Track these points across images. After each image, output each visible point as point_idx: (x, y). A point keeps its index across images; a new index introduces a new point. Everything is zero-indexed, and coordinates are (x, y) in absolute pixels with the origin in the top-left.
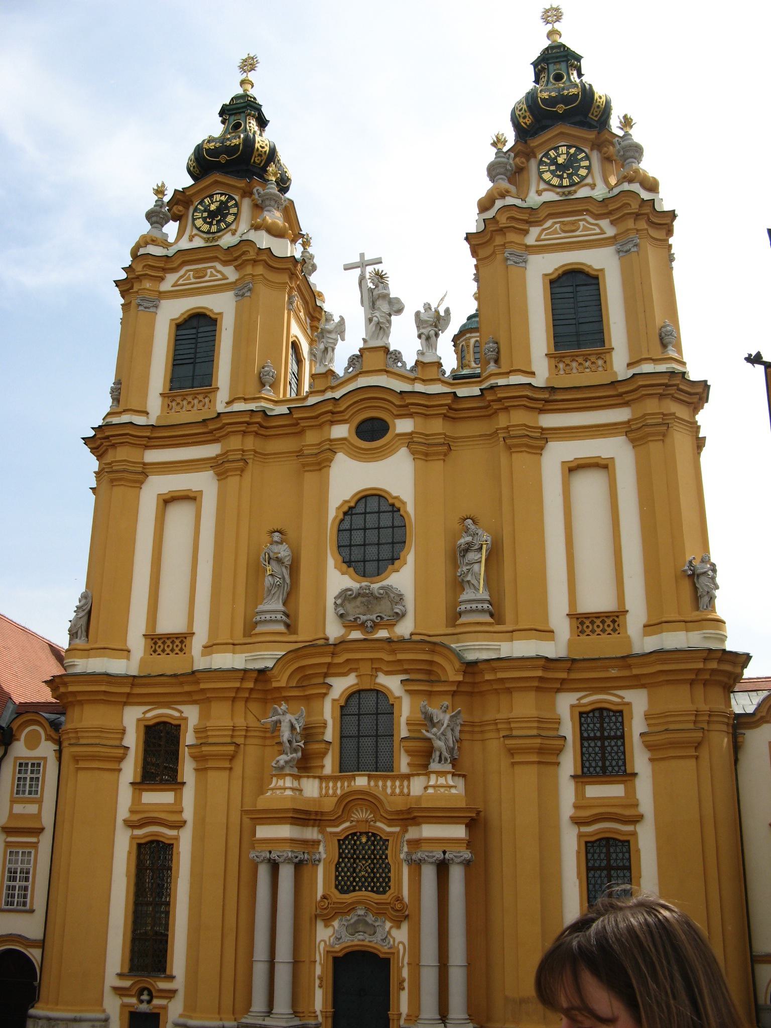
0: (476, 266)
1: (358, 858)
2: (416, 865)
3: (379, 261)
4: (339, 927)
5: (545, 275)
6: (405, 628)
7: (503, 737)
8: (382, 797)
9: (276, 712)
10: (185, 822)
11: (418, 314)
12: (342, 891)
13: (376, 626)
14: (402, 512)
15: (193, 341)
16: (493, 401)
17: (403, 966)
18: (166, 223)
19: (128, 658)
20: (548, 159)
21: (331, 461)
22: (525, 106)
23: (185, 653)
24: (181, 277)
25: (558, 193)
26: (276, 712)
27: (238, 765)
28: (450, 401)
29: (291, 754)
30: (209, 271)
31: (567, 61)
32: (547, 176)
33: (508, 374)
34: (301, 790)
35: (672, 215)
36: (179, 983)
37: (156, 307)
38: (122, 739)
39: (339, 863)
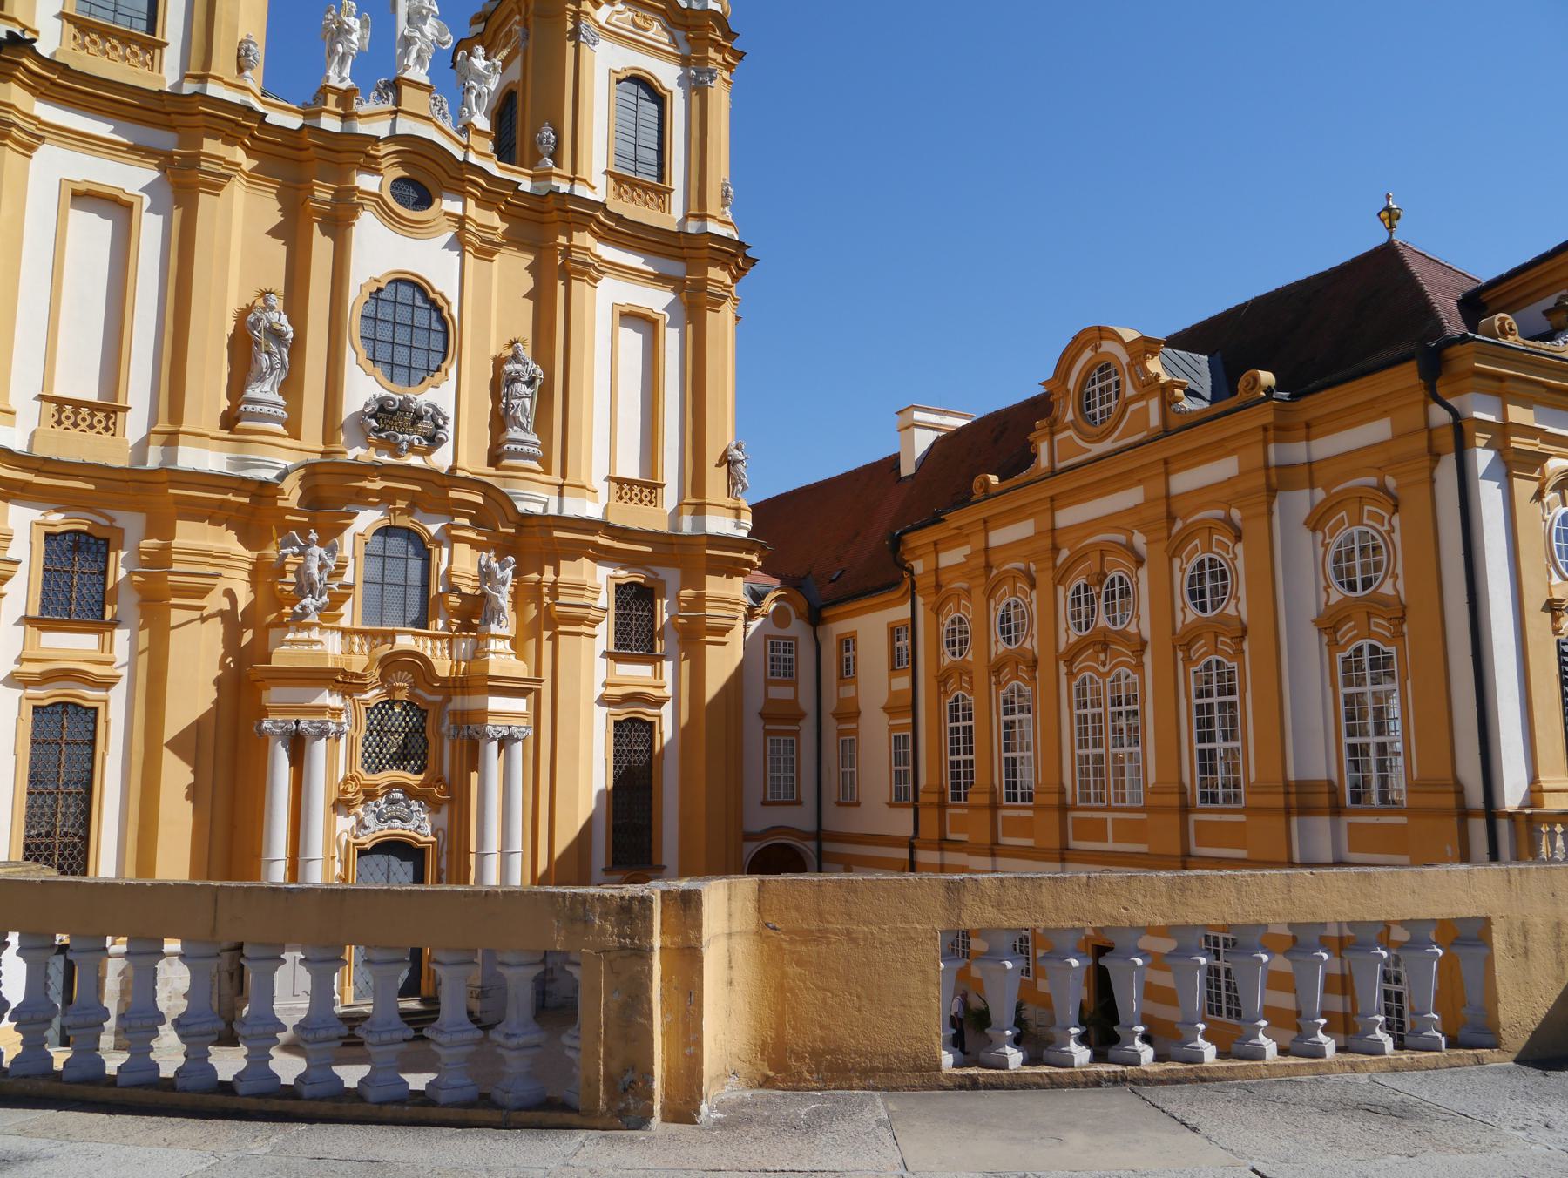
1: (390, 731)
6: (441, 459)
13: (412, 449)
14: (445, 314)
17: (442, 855)
23: (113, 435)
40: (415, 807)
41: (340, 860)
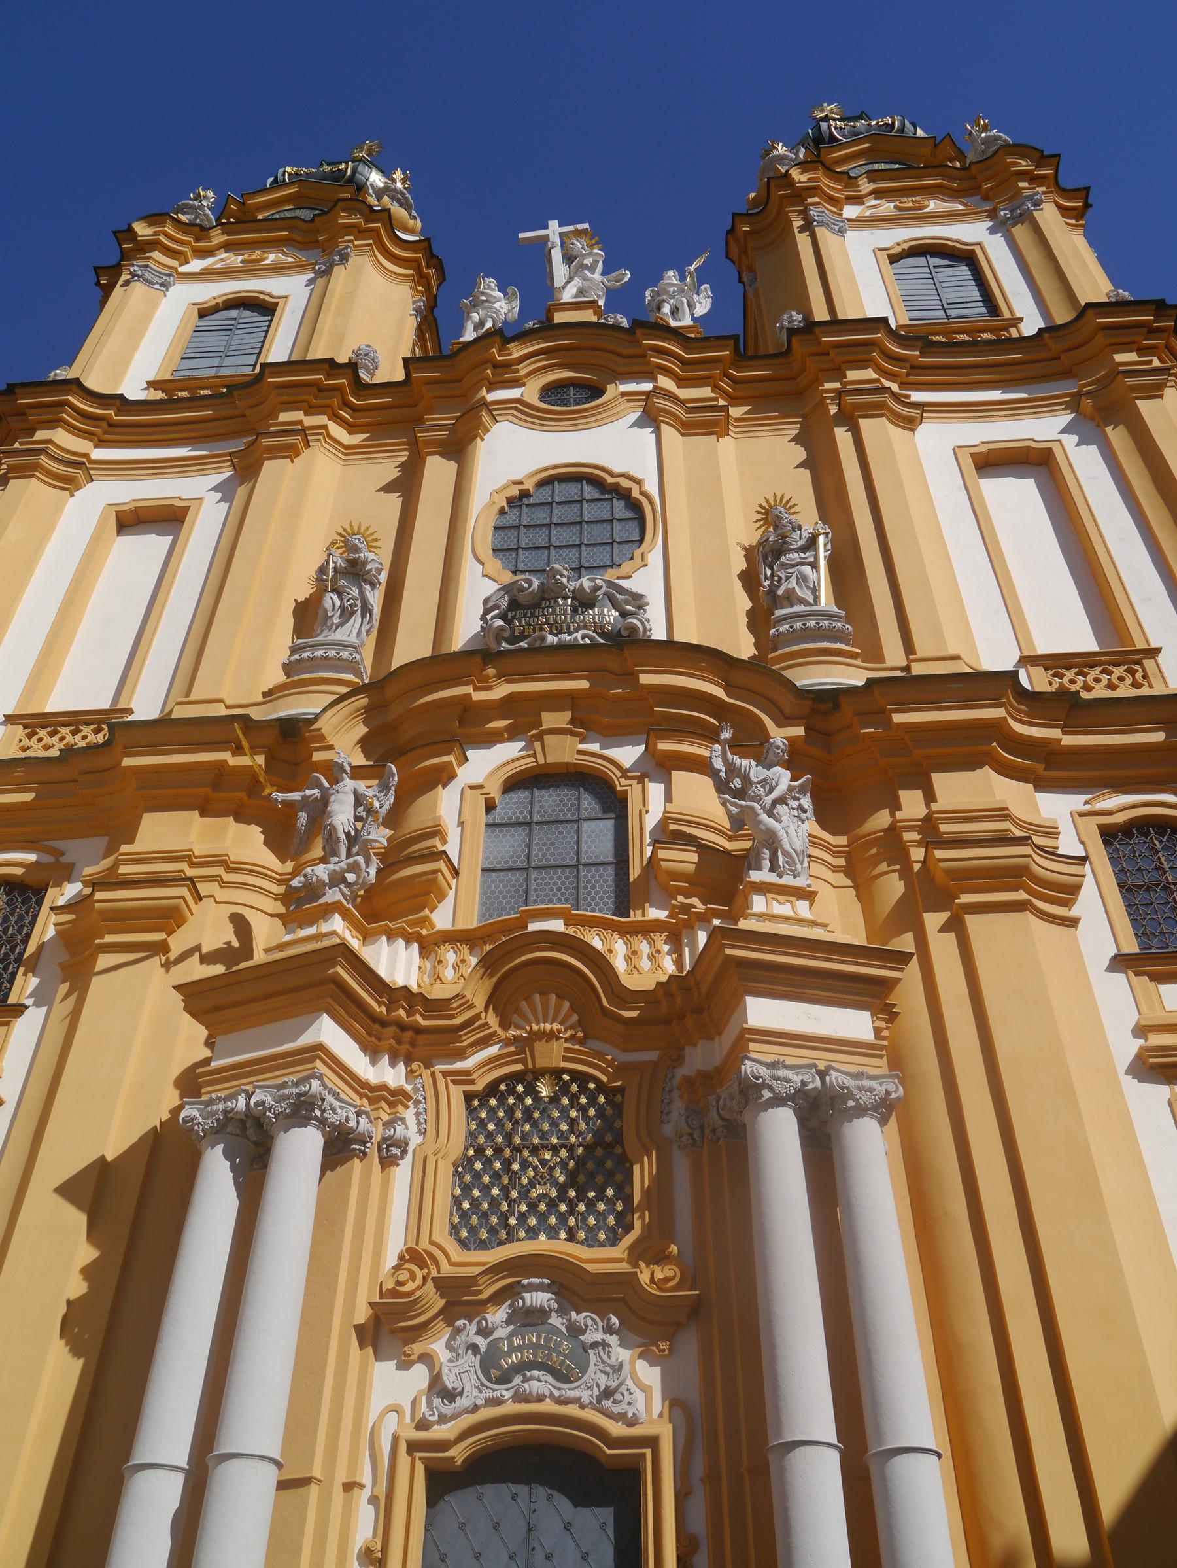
14: (635, 493)
15: (229, 333)
40: (594, 1335)
41: (373, 1500)
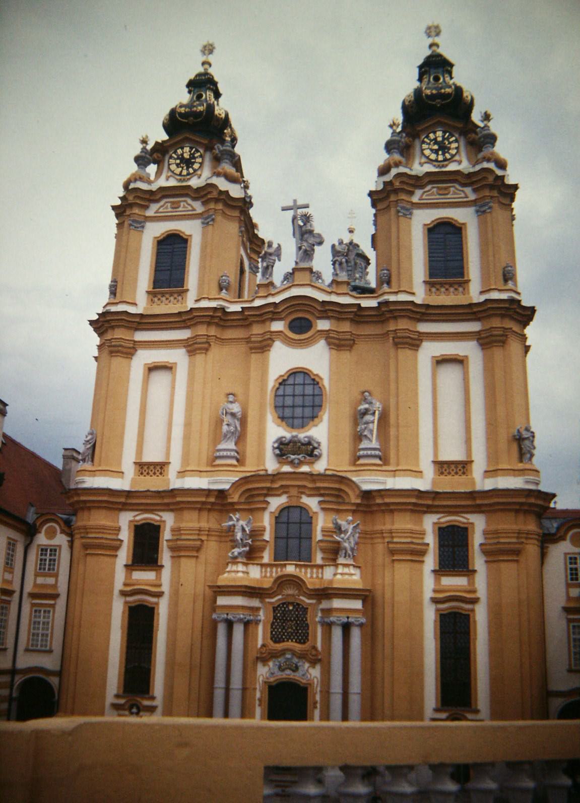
0: (375, 215)
1: (286, 619)
2: (328, 626)
3: (307, 206)
4: (273, 666)
5: (425, 225)
7: (388, 542)
8: (304, 579)
9: (231, 519)
10: (163, 593)
11: (333, 246)
12: (275, 642)
13: (301, 463)
14: (320, 385)
16: (386, 311)
17: (316, 693)
18: (149, 164)
19: (122, 478)
20: (429, 140)
21: (270, 346)
22: (413, 99)
24: (161, 206)
25: (435, 166)
26: (231, 519)
27: (202, 556)
28: (356, 310)
29: (242, 547)
30: (182, 204)
31: (444, 67)
32: (427, 152)
33: (396, 293)
34: (248, 573)
35: (515, 187)
36: (158, 702)
37: (143, 227)
38: (118, 534)
39: (273, 624)
